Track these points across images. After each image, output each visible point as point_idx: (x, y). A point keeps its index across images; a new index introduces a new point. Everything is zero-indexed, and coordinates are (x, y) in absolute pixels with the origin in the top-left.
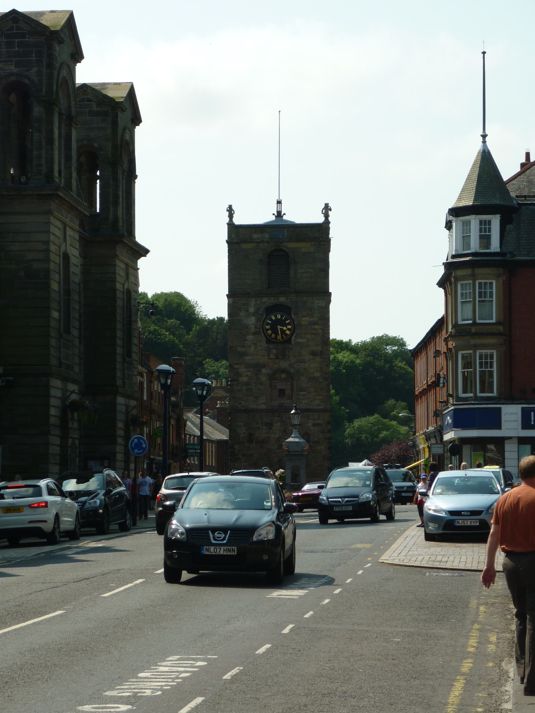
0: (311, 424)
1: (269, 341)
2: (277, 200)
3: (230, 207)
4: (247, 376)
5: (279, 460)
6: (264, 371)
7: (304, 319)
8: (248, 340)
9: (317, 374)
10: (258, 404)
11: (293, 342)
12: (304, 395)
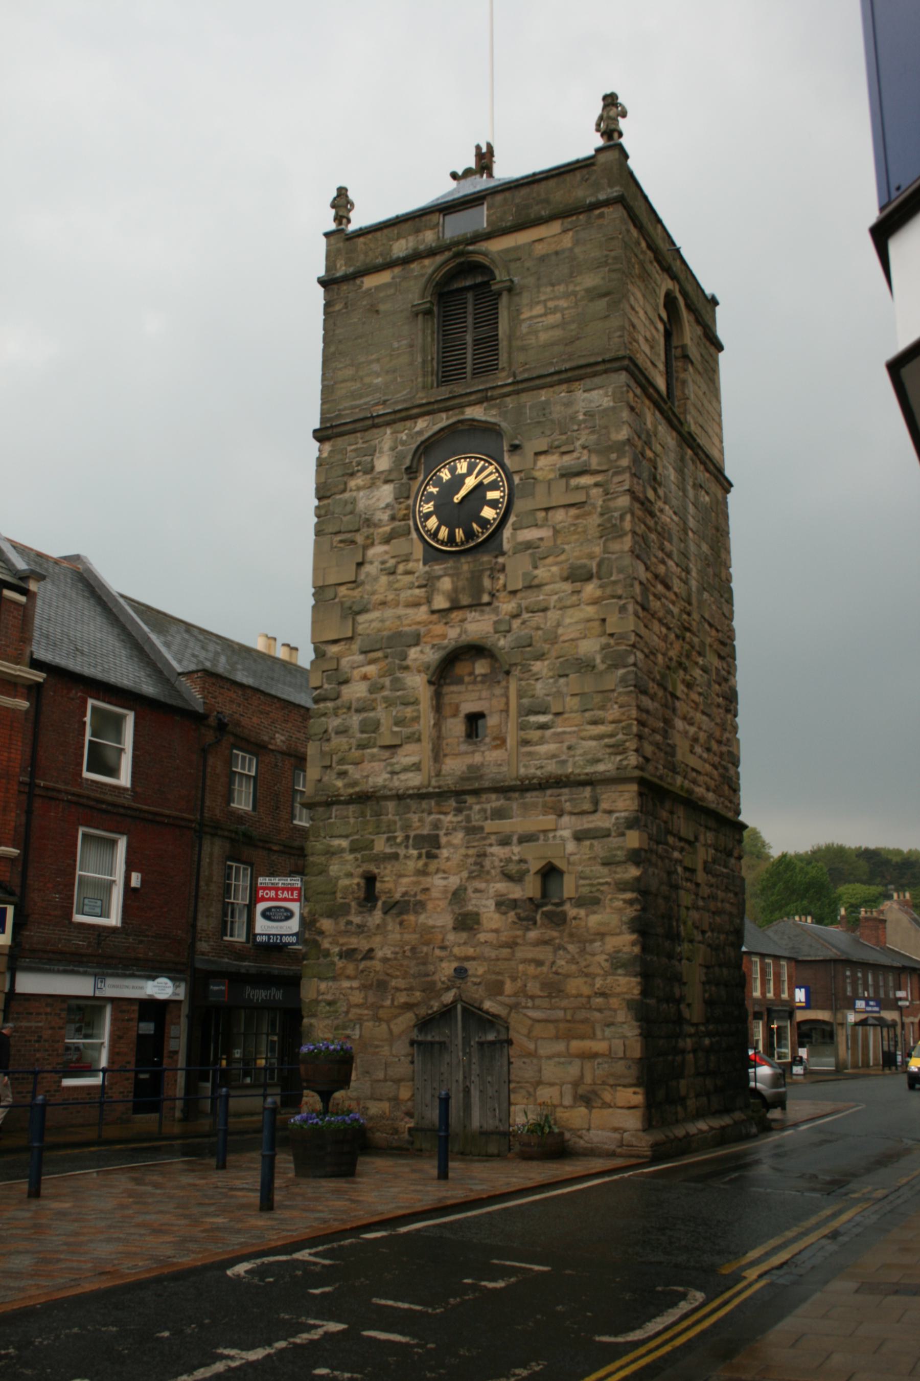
0: (566, 833)
1: (432, 554)
2: (478, 148)
3: (342, 192)
4: (365, 678)
5: (455, 970)
6: (413, 653)
7: (543, 461)
8: (371, 563)
9: (590, 647)
10: (393, 773)
11: (506, 546)
12: (543, 727)
